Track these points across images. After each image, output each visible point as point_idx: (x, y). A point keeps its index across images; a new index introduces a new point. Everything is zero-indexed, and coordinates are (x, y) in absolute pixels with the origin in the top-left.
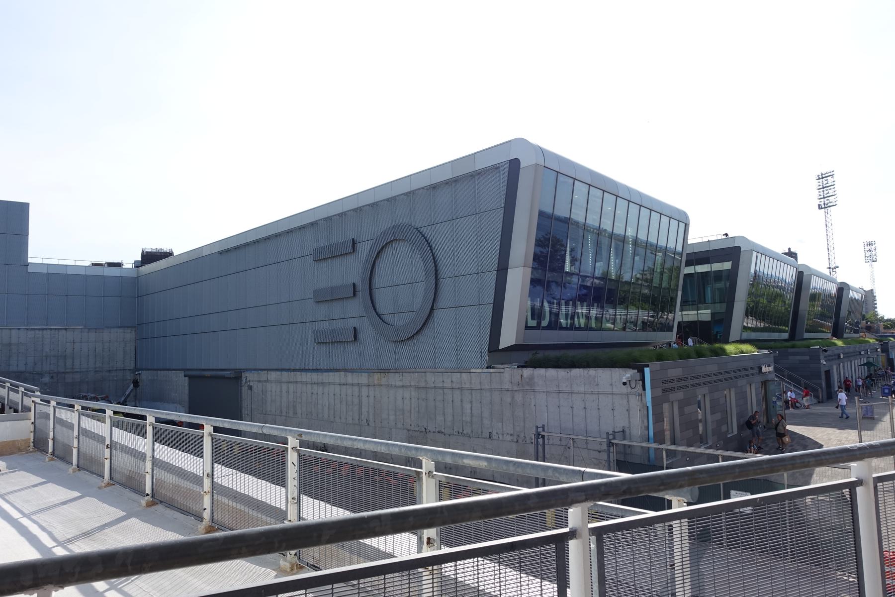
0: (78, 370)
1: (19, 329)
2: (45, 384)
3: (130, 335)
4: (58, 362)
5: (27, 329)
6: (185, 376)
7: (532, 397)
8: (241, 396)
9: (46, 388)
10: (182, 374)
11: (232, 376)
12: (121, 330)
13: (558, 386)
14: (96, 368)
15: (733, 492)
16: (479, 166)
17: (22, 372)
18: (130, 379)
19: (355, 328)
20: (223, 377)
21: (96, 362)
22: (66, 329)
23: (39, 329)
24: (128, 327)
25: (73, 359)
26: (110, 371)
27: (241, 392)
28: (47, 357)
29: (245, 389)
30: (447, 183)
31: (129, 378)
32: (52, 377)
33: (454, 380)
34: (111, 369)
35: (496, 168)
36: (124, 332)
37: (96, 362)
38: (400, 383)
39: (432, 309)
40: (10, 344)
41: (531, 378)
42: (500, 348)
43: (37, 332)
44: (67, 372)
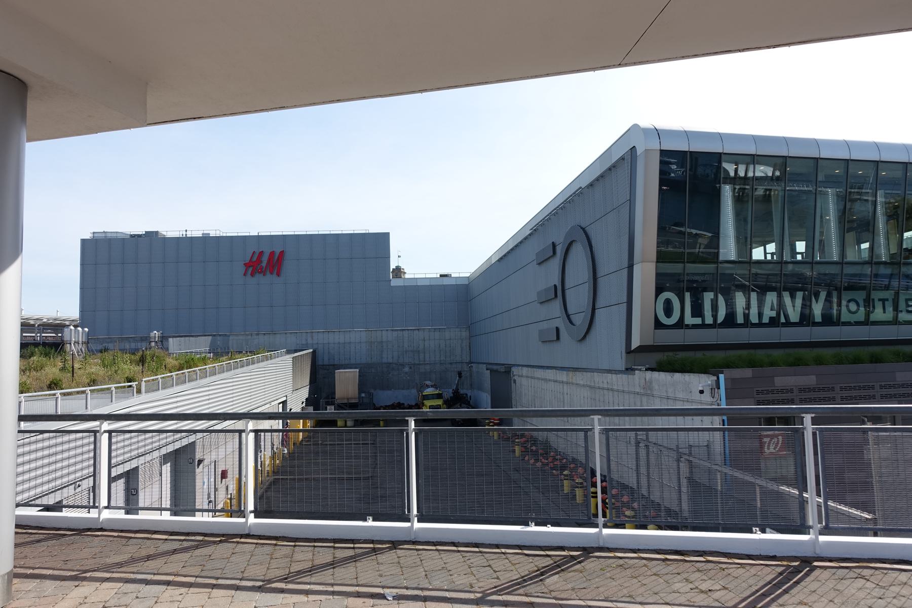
0: (429, 362)
1: (387, 330)
2: (406, 373)
3: (465, 334)
4: (414, 355)
5: (392, 330)
6: (487, 369)
7: (652, 403)
9: (406, 376)
11: (503, 370)
13: (667, 391)
14: (441, 361)
15: (768, 530)
16: (615, 158)
17: (391, 363)
18: (467, 371)
19: (557, 328)
21: (440, 356)
22: (418, 329)
23: (401, 330)
25: (424, 353)
26: (451, 363)
28: (406, 351)
29: (512, 382)
30: (597, 179)
31: (466, 370)
32: (411, 368)
33: (608, 381)
34: (452, 362)
35: (622, 159)
36: (461, 331)
37: (440, 356)
38: (581, 383)
39: (594, 309)
40: (382, 342)
41: (651, 382)
42: (632, 349)
43: (399, 332)
44: (421, 364)
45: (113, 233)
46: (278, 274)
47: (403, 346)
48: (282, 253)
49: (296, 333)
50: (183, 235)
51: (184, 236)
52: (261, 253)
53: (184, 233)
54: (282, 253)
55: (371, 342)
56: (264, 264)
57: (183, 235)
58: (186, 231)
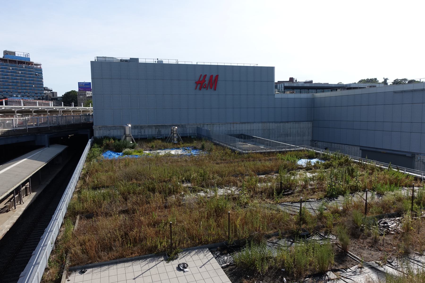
3: (310, 125)
8: (414, 165)
10: (359, 148)
12: (307, 123)
20: (405, 156)
24: (310, 121)
27: (414, 164)
40: (270, 129)
45: (110, 58)
46: (215, 89)
47: (280, 132)
48: (217, 76)
49: (225, 124)
50: (155, 62)
51: (157, 63)
52: (206, 76)
53: (157, 61)
54: (217, 76)
55: (264, 129)
56: (207, 83)
57: (155, 62)
58: (158, 59)
